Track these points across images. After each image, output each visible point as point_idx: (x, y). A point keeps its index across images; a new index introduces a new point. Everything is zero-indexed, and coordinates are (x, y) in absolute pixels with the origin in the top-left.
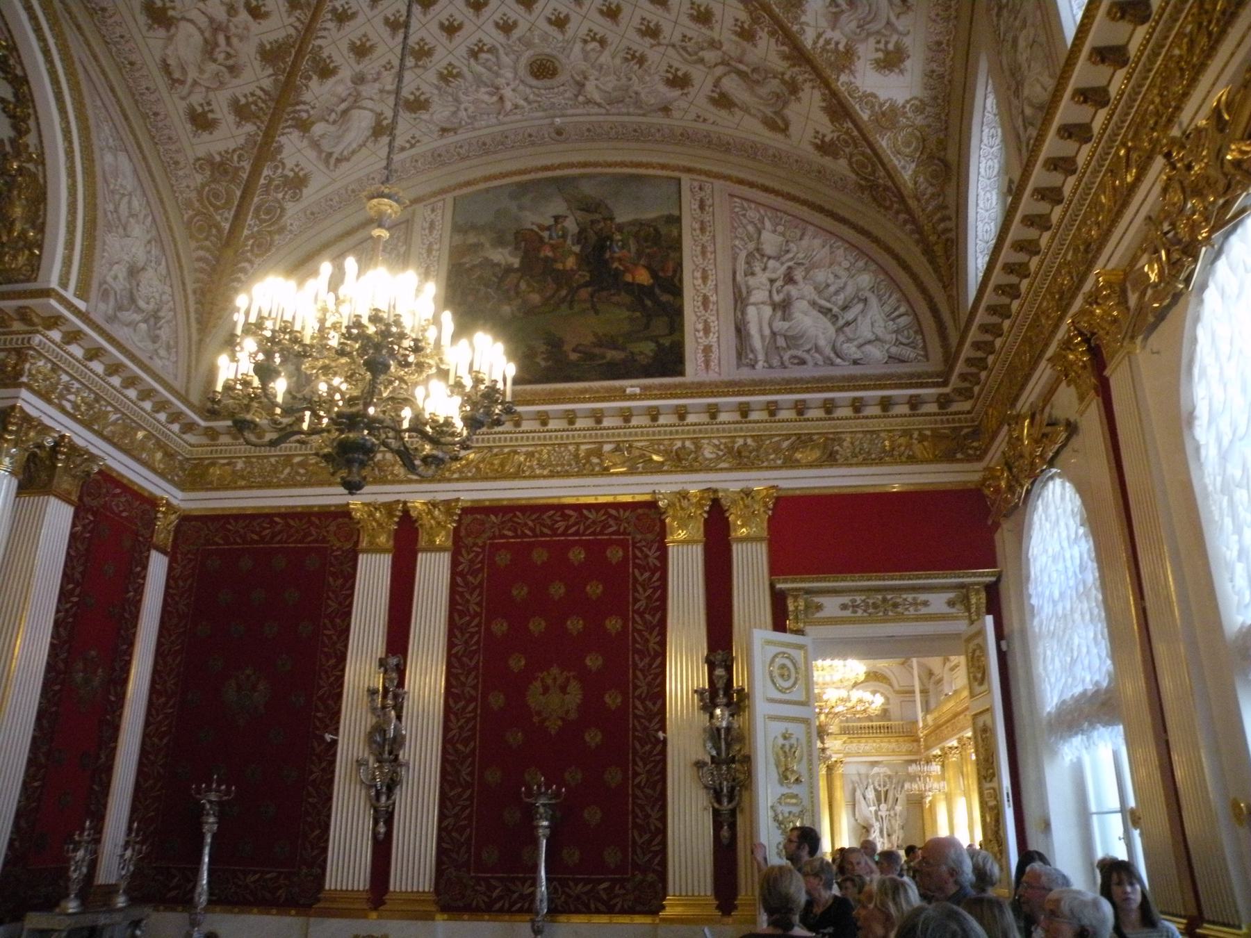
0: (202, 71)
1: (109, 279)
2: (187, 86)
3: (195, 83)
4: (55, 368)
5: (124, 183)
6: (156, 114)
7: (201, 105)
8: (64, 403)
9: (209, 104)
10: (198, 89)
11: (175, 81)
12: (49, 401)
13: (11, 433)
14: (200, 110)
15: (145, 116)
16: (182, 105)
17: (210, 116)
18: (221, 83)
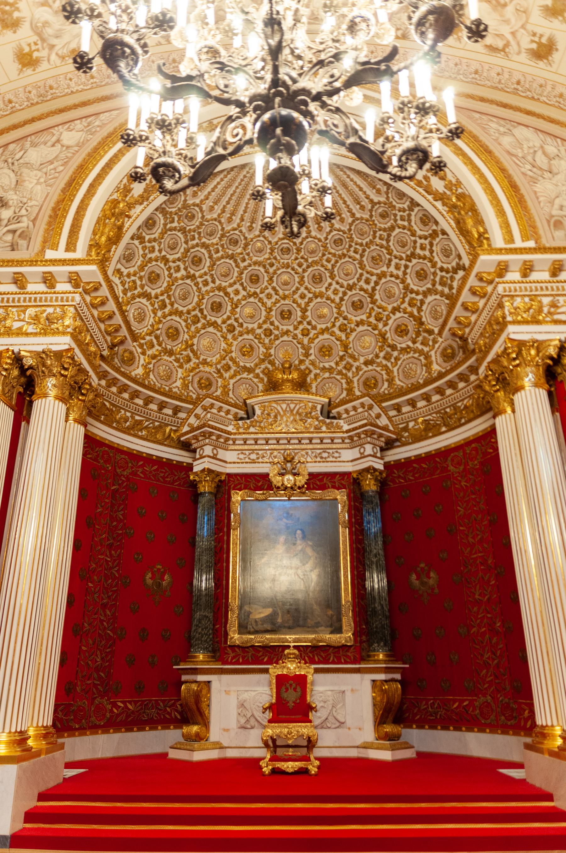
0: (507, 22)
1: (554, 212)
2: (513, 42)
3: (513, 34)
4: (532, 298)
5: (531, 144)
6: (518, 83)
7: (533, 41)
8: (556, 317)
9: (534, 35)
10: (518, 35)
11: (503, 50)
12: (538, 322)
13: (514, 359)
14: (534, 46)
15: (515, 92)
16: (524, 57)
17: (544, 40)
18: (524, 12)
